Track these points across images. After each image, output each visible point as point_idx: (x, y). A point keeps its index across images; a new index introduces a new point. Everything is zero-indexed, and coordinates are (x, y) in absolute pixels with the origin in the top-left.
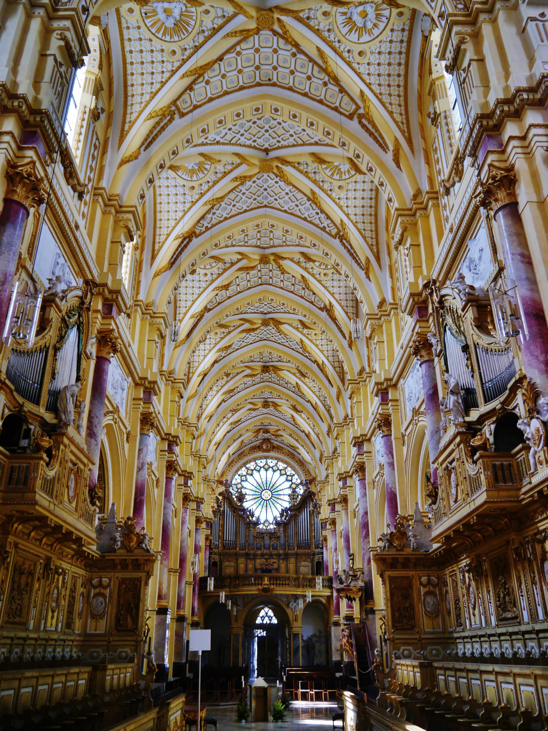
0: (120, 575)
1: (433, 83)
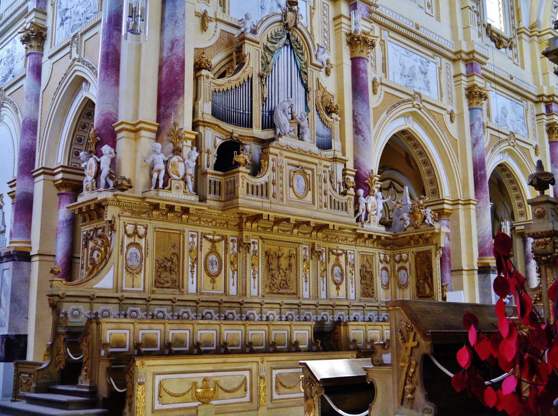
0: (415, 250)
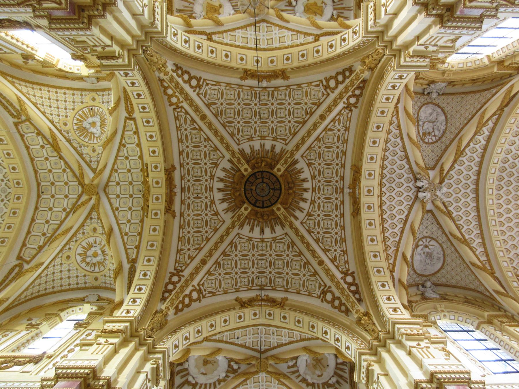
1: (58, 315)
